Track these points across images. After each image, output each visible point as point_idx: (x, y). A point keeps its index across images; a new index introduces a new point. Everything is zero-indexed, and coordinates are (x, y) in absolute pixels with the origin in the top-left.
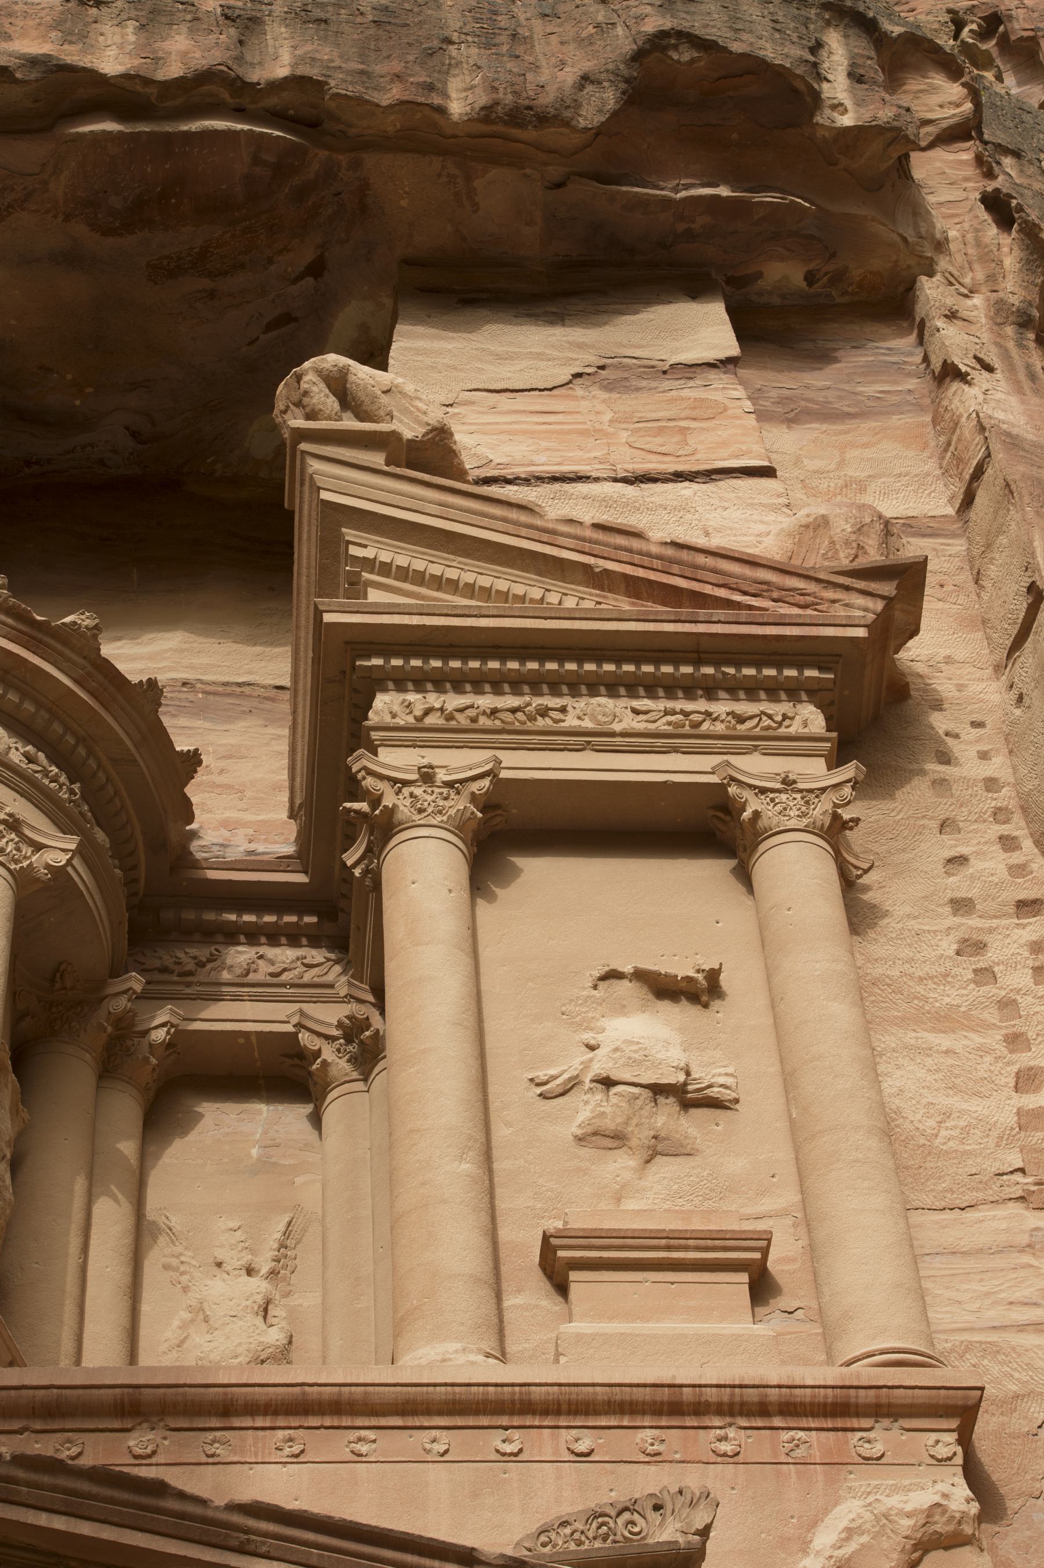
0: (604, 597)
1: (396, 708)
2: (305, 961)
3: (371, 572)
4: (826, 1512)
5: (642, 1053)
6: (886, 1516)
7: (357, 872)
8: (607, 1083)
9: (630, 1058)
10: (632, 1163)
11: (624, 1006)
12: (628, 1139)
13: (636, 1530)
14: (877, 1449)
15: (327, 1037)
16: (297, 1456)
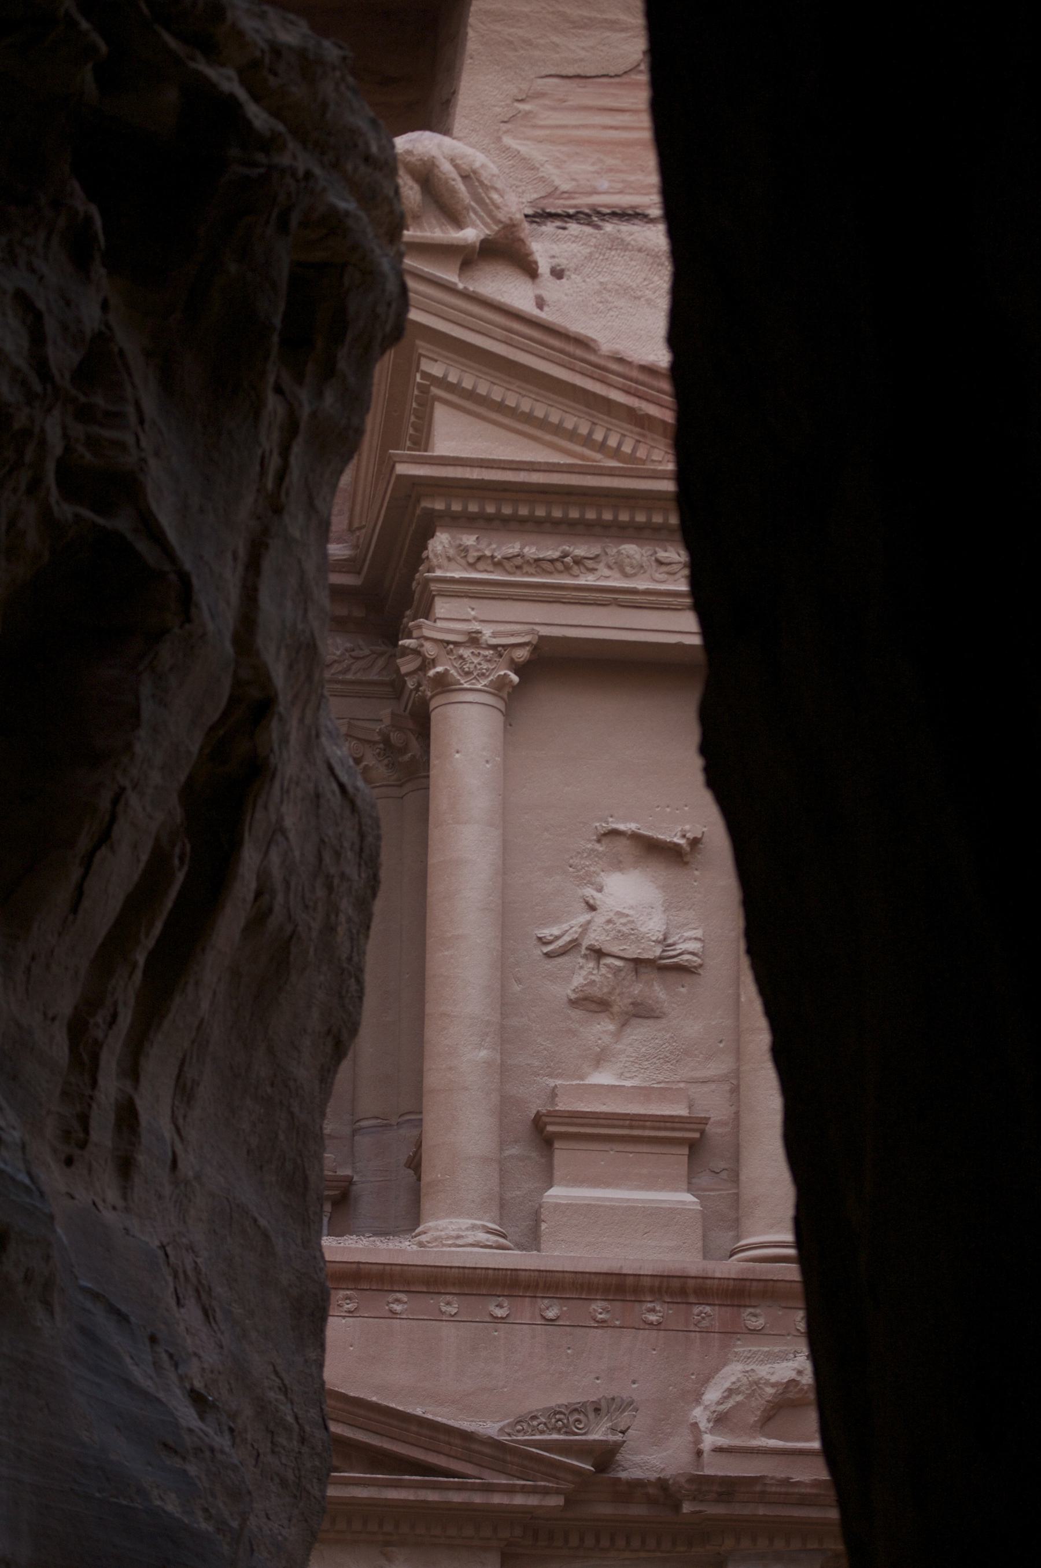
0: (644, 436)
1: (452, 552)
2: (353, 654)
3: (439, 387)
4: (717, 1370)
5: (630, 926)
6: (756, 1383)
7: (410, 684)
8: (598, 954)
9: (619, 931)
10: (611, 1027)
11: (620, 862)
12: (611, 1006)
13: (580, 1426)
14: (759, 1323)
15: (369, 742)
16: (350, 1312)
